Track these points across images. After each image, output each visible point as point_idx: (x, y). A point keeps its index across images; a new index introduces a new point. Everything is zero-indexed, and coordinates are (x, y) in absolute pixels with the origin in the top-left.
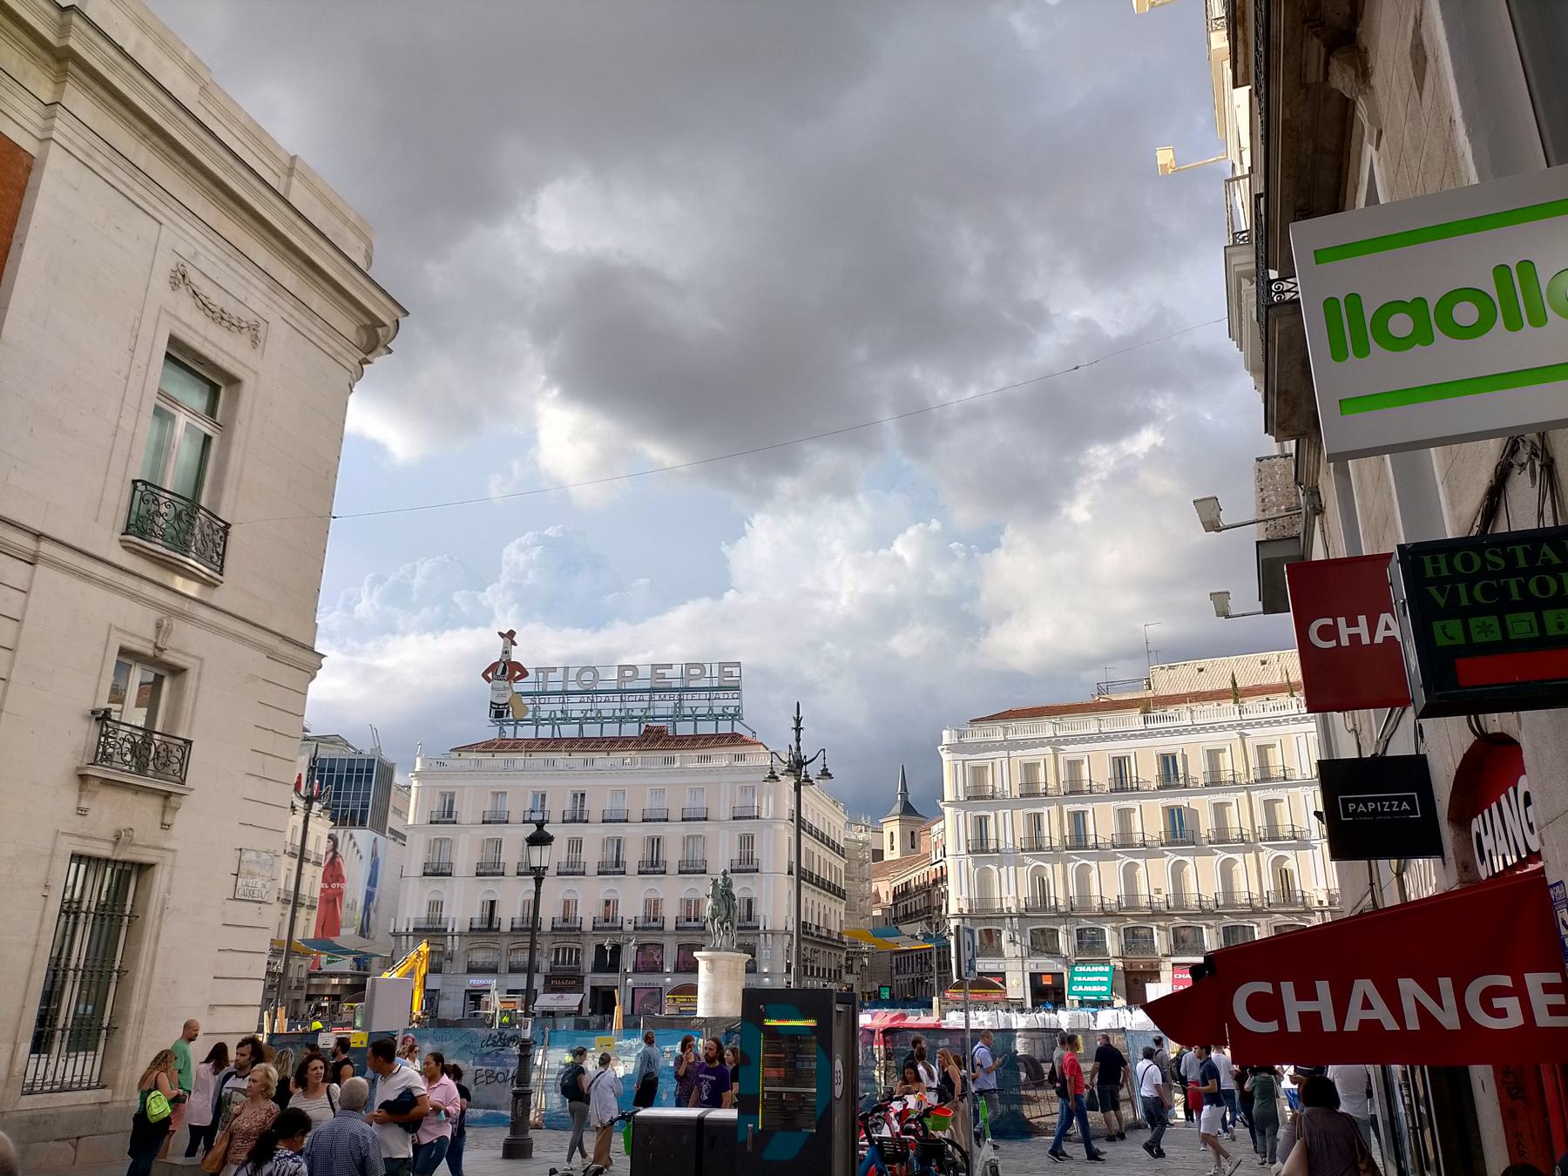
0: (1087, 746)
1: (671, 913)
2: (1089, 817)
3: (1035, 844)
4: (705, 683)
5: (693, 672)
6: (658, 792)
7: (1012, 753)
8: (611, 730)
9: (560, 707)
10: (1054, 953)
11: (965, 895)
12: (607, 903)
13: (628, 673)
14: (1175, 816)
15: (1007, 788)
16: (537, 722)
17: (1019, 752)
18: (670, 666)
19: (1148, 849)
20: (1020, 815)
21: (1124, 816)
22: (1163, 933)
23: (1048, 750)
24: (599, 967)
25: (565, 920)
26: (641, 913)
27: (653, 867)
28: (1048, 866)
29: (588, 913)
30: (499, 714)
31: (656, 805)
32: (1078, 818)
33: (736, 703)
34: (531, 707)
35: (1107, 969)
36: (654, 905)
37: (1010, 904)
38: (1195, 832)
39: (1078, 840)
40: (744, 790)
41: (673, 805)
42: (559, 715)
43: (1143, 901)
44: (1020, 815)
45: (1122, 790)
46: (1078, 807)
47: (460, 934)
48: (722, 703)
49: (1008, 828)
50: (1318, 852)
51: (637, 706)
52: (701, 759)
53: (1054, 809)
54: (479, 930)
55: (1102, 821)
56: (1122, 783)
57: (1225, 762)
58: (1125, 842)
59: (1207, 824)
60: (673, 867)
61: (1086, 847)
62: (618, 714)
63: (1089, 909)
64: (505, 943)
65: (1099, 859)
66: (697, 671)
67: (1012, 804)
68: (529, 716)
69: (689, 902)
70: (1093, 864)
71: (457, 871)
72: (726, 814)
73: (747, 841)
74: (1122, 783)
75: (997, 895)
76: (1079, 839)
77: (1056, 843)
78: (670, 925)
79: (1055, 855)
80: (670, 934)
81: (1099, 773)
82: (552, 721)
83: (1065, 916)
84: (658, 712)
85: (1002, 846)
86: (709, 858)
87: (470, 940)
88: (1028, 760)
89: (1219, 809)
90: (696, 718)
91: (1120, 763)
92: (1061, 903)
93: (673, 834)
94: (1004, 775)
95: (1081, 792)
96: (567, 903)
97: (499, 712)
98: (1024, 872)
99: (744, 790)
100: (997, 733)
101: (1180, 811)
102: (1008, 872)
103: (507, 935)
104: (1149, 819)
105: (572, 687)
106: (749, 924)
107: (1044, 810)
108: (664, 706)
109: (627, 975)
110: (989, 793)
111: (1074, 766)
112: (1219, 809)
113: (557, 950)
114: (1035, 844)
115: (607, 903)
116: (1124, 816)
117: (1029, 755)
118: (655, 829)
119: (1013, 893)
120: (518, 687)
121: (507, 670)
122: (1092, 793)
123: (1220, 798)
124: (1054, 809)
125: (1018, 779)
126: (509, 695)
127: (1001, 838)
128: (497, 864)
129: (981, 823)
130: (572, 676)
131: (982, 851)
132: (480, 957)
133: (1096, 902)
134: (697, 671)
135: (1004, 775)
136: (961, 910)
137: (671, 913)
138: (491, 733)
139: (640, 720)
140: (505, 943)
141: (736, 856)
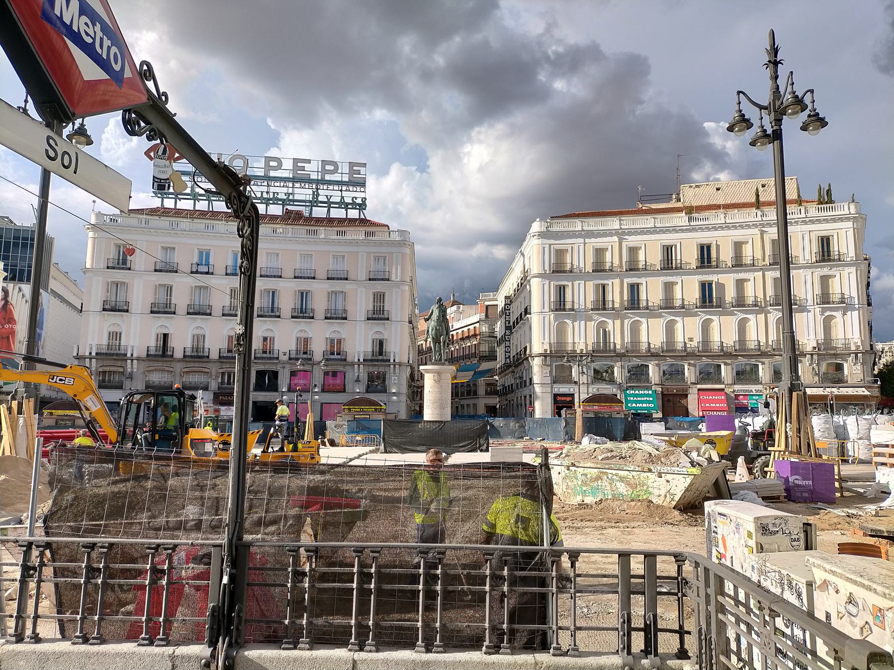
0: (645, 237)
1: (318, 349)
2: (643, 289)
3: (601, 305)
4: (336, 177)
5: (327, 167)
6: (306, 256)
7: (587, 240)
10: (612, 381)
11: (547, 340)
12: (265, 339)
13: (272, 164)
14: (706, 287)
15: (582, 265)
16: (195, 197)
17: (593, 240)
18: (309, 161)
19: (685, 310)
20: (590, 285)
21: (668, 287)
22: (692, 368)
23: (616, 239)
25: (229, 351)
26: (294, 348)
27: (303, 313)
28: (610, 322)
32: (634, 289)
33: (363, 195)
34: (189, 184)
35: (650, 392)
36: (304, 344)
37: (580, 347)
38: (721, 299)
39: (634, 302)
40: (377, 259)
43: (680, 346)
44: (590, 285)
45: (668, 269)
46: (635, 280)
47: (138, 359)
49: (582, 294)
50: (811, 315)
51: (281, 191)
52: (338, 233)
53: (617, 282)
54: (155, 356)
55: (652, 291)
56: (669, 263)
57: (748, 252)
58: (668, 304)
59: (730, 294)
60: (320, 313)
61: (639, 308)
62: (265, 195)
63: (638, 351)
64: (178, 367)
65: (648, 317)
66: (332, 168)
67: (583, 276)
68: (188, 191)
69: (332, 340)
70: (644, 320)
71: (133, 308)
72: (363, 275)
73: (379, 297)
74: (669, 263)
75: (570, 340)
76: (633, 303)
77: (617, 305)
78: (318, 356)
79: (616, 314)
81: (652, 256)
83: (621, 356)
84: (297, 197)
85: (576, 307)
86: (348, 308)
88: (599, 246)
89: (740, 284)
90: (329, 204)
91: (668, 250)
92: (618, 347)
93: (320, 292)
94: (580, 256)
95: (638, 270)
98: (592, 325)
100: (577, 225)
101: (710, 284)
102: (580, 325)
103: (179, 360)
104: (688, 289)
106: (380, 358)
107: (609, 282)
108: (303, 193)
109: (283, 393)
110: (568, 267)
111: (633, 251)
112: (740, 284)
113: (223, 374)
114: (601, 305)
115: (265, 339)
116: (668, 287)
117: (600, 242)
118: (304, 285)
119: (583, 340)
122: (647, 270)
123: (742, 276)
124: (617, 282)
125: (590, 259)
126: (170, 172)
127: (576, 300)
128: (168, 304)
129: (561, 290)
131: (560, 310)
133: (644, 347)
134: (332, 168)
135: (580, 256)
136: (546, 351)
137: (318, 349)
139: (284, 202)
141: (371, 308)
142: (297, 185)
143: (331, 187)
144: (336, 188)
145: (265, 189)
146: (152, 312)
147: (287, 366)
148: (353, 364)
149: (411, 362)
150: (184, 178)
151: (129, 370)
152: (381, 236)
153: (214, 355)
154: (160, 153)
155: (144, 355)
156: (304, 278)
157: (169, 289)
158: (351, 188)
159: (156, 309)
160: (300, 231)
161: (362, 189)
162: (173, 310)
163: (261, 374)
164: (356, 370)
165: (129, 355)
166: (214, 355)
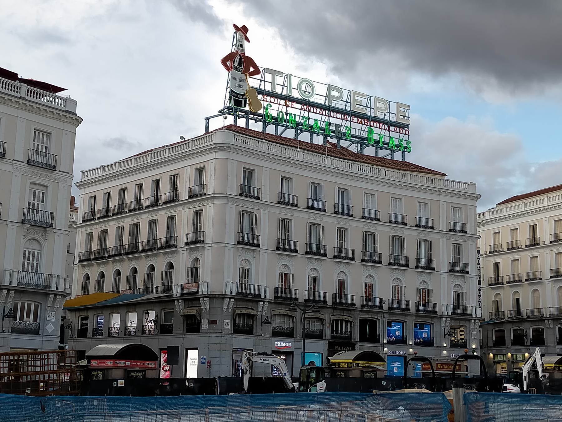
16: (265, 119)
36: (399, 290)
41: (410, 210)
48: (395, 136)
82: (276, 121)
87: (273, 306)
105: (295, 94)
120: (253, 82)
130: (294, 84)
147: (386, 315)
148: (441, 317)
150: (260, 97)
152: (439, 184)
153: (301, 300)
154: (236, 64)
164: (443, 325)
166: (301, 300)
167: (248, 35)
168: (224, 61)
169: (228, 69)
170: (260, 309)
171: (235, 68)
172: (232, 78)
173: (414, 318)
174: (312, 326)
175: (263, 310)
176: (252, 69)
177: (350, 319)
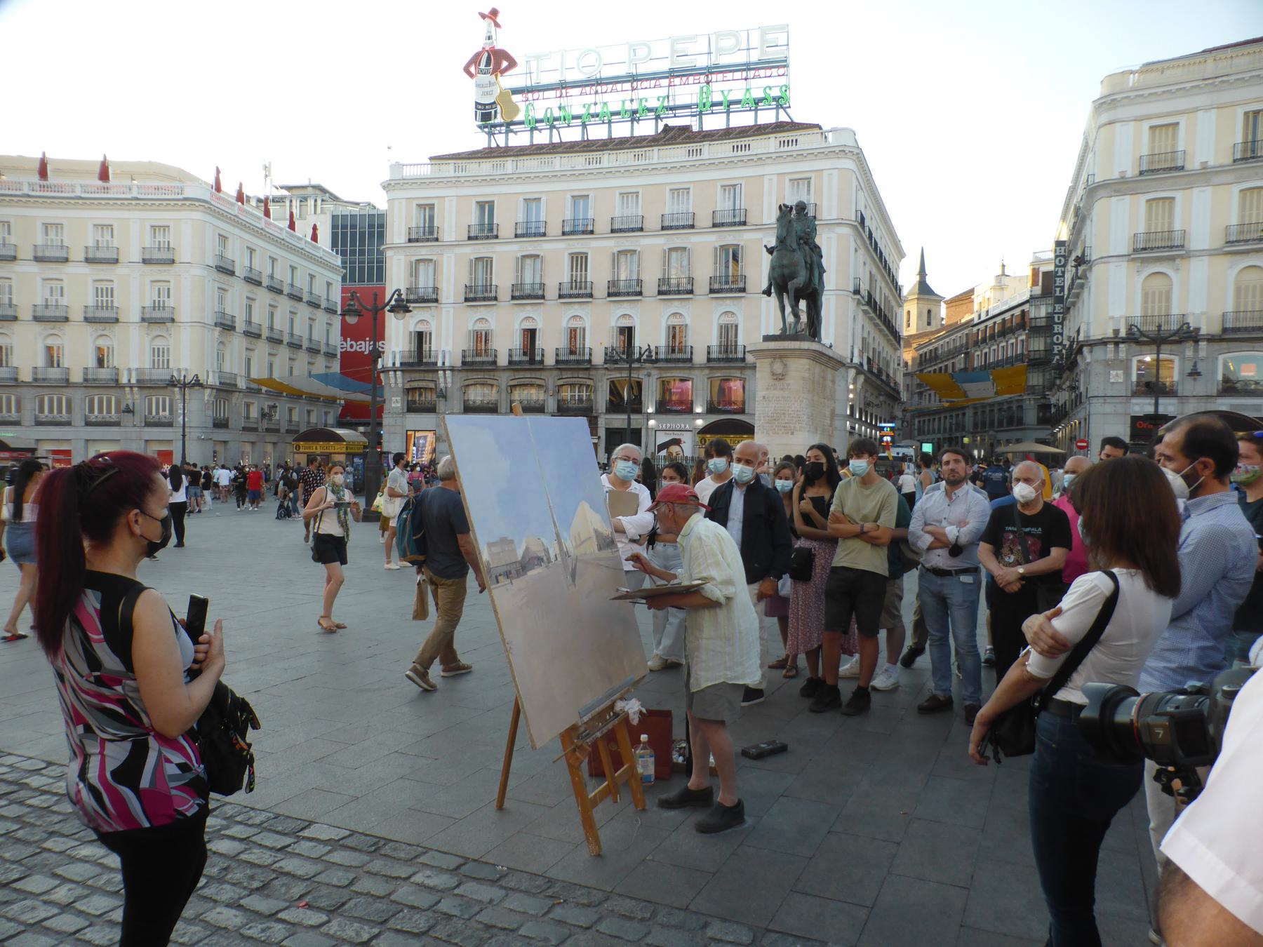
8: (621, 130)
9: (556, 103)
24: (615, 405)
25: (572, 352)
29: (598, 342)
30: (486, 117)
31: (682, 208)
34: (522, 106)
42: (557, 113)
47: (452, 369)
51: (651, 96)
64: (504, 379)
80: (701, 368)
87: (464, 375)
96: (573, 333)
97: (485, 115)
99: (796, 182)
103: (505, 369)
108: (687, 93)
109: (649, 416)
120: (509, 81)
121: (495, 60)
132: (477, 395)
138: (480, 141)
140: (504, 379)
142: (677, 81)
143: (729, 76)
144: (737, 75)
145: (628, 95)
146: (467, 300)
149: (856, 360)
150: (515, 98)
151: (442, 385)
154: (482, 66)
155: (458, 364)
156: (677, 228)
157: (487, 262)
158: (762, 73)
159: (517, 294)
160: (677, 153)
161: (781, 71)
162: (493, 294)
163: (614, 391)
165: (440, 364)
167: (498, 20)
168: (467, 70)
169: (471, 75)
170: (442, 380)
171: (482, 72)
172: (478, 86)
173: (707, 372)
174: (533, 395)
175: (445, 380)
176: (505, 64)
177: (589, 382)
